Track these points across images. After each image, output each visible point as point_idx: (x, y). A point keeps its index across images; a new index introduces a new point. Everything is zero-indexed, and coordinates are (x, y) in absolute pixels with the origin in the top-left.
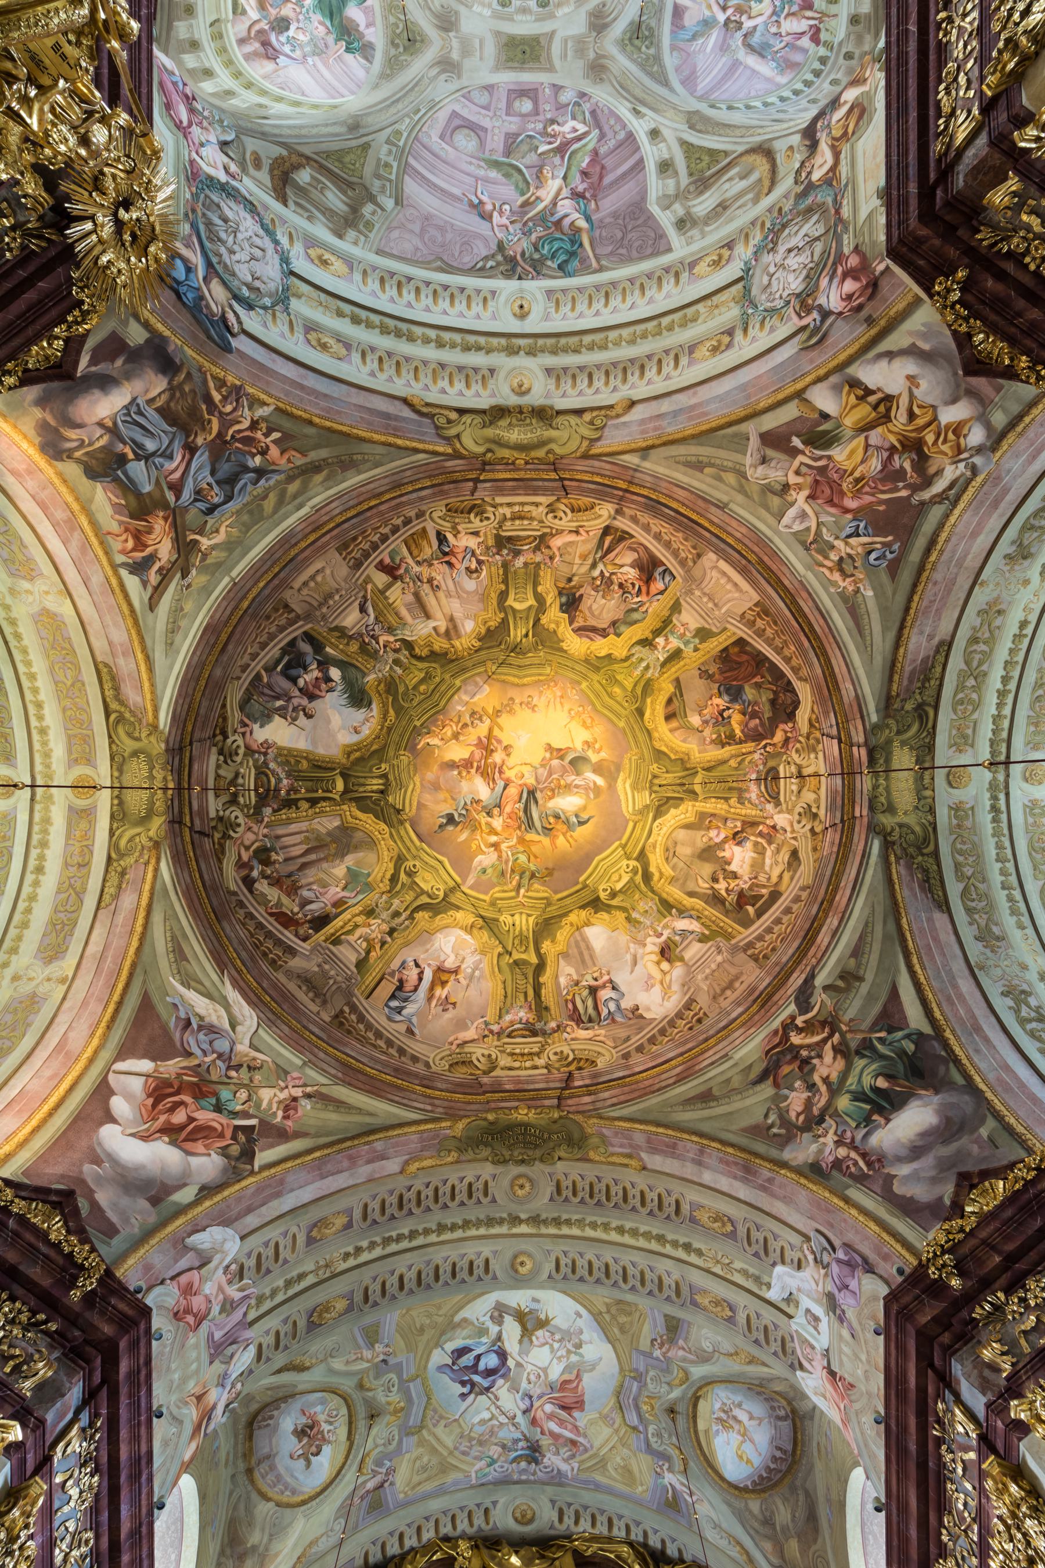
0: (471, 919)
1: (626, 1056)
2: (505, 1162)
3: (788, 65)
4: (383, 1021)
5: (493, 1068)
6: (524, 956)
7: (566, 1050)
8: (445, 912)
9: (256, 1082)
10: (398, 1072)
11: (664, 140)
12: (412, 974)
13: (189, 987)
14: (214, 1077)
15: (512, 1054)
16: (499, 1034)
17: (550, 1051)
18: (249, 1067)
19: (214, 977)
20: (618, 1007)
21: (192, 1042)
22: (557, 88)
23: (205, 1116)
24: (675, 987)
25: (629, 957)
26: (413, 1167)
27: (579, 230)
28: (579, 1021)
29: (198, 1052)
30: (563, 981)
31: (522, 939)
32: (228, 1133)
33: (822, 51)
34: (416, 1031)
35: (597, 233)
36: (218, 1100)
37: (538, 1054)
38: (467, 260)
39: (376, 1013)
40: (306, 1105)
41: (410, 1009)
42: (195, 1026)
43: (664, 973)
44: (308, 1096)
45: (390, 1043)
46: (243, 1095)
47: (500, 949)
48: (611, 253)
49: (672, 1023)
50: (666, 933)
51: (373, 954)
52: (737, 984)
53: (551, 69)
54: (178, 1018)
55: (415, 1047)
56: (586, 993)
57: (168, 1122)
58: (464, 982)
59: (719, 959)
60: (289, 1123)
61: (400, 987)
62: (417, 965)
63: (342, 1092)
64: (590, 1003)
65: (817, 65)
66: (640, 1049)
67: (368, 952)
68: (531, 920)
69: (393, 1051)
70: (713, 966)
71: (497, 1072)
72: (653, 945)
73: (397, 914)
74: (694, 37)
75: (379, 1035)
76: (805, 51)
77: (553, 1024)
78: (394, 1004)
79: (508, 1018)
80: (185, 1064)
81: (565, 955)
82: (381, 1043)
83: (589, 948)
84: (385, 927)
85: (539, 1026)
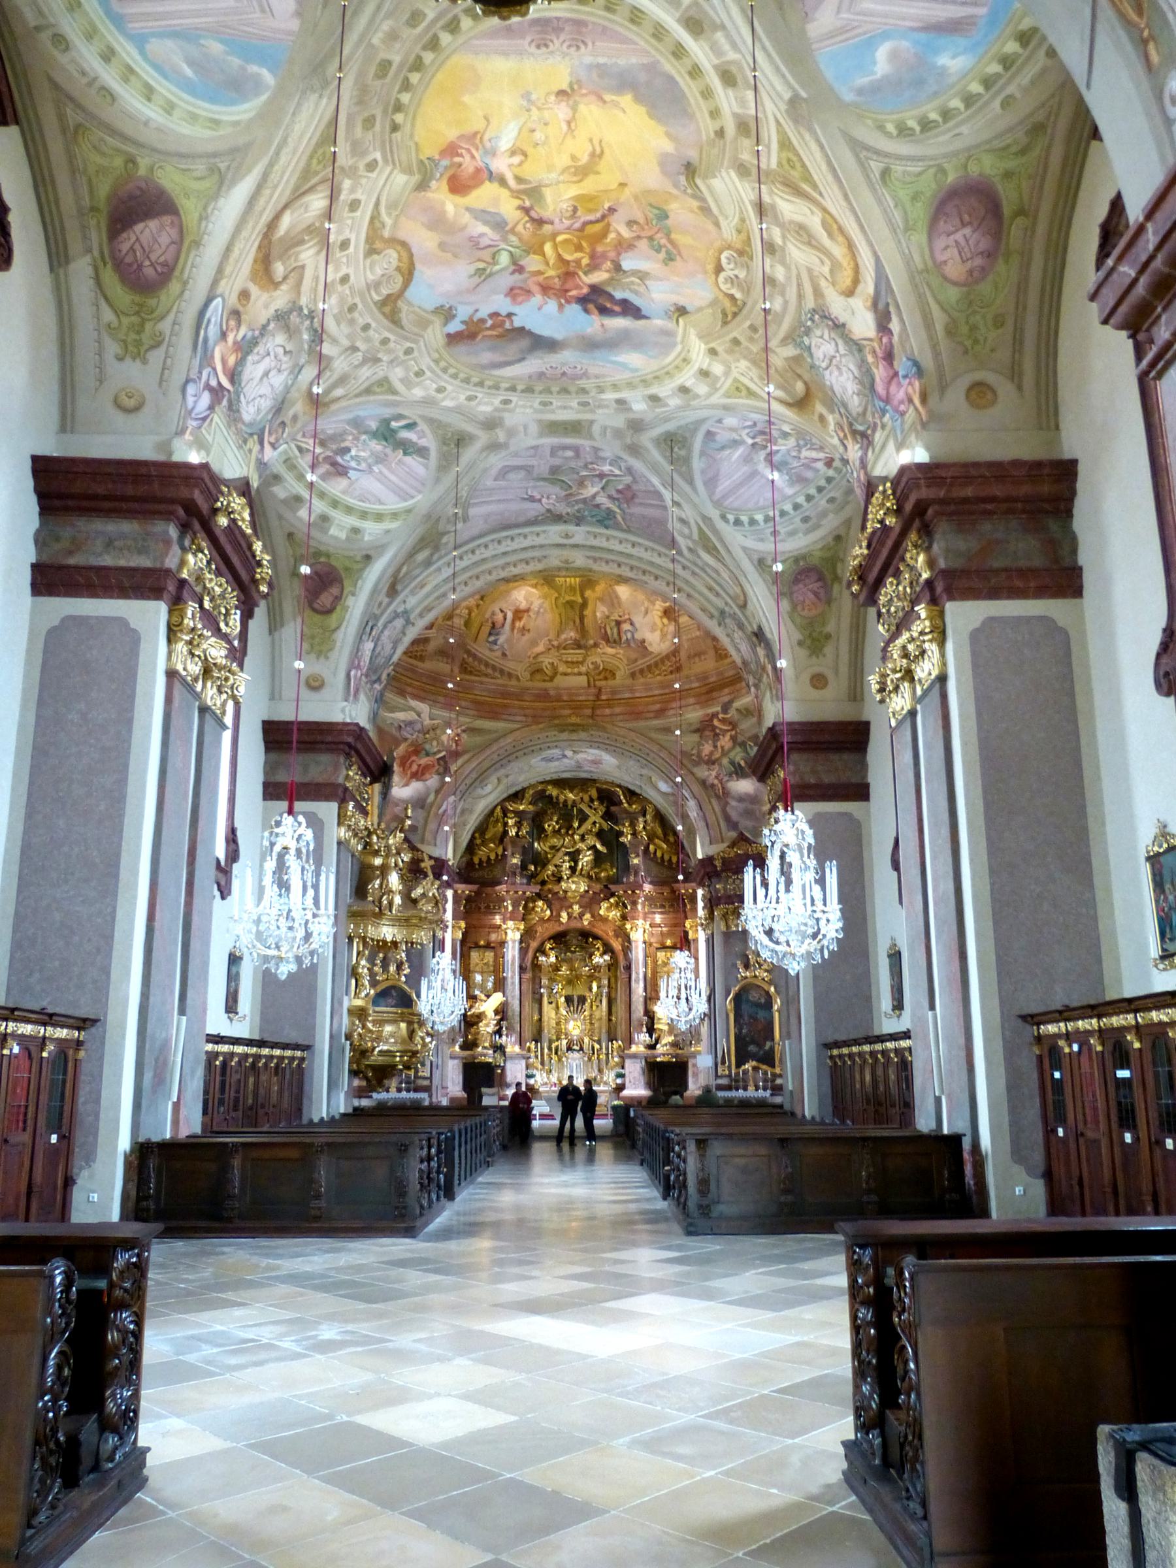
3: (799, 480)
4: (487, 653)
5: (555, 674)
7: (599, 661)
10: (505, 695)
12: (500, 616)
16: (558, 648)
22: (596, 450)
23: (424, 761)
28: (608, 641)
31: (572, 589)
33: (831, 473)
37: (582, 663)
38: (521, 519)
39: (482, 650)
40: (464, 736)
41: (502, 639)
45: (494, 668)
49: (662, 661)
53: (591, 438)
55: (510, 665)
61: (494, 625)
63: (480, 723)
65: (823, 483)
66: (642, 671)
69: (497, 674)
71: (560, 681)
72: (659, 605)
74: (723, 448)
75: (487, 665)
76: (817, 471)
77: (591, 642)
78: (492, 639)
79: (563, 637)
81: (601, 599)
82: (490, 671)
83: (617, 597)
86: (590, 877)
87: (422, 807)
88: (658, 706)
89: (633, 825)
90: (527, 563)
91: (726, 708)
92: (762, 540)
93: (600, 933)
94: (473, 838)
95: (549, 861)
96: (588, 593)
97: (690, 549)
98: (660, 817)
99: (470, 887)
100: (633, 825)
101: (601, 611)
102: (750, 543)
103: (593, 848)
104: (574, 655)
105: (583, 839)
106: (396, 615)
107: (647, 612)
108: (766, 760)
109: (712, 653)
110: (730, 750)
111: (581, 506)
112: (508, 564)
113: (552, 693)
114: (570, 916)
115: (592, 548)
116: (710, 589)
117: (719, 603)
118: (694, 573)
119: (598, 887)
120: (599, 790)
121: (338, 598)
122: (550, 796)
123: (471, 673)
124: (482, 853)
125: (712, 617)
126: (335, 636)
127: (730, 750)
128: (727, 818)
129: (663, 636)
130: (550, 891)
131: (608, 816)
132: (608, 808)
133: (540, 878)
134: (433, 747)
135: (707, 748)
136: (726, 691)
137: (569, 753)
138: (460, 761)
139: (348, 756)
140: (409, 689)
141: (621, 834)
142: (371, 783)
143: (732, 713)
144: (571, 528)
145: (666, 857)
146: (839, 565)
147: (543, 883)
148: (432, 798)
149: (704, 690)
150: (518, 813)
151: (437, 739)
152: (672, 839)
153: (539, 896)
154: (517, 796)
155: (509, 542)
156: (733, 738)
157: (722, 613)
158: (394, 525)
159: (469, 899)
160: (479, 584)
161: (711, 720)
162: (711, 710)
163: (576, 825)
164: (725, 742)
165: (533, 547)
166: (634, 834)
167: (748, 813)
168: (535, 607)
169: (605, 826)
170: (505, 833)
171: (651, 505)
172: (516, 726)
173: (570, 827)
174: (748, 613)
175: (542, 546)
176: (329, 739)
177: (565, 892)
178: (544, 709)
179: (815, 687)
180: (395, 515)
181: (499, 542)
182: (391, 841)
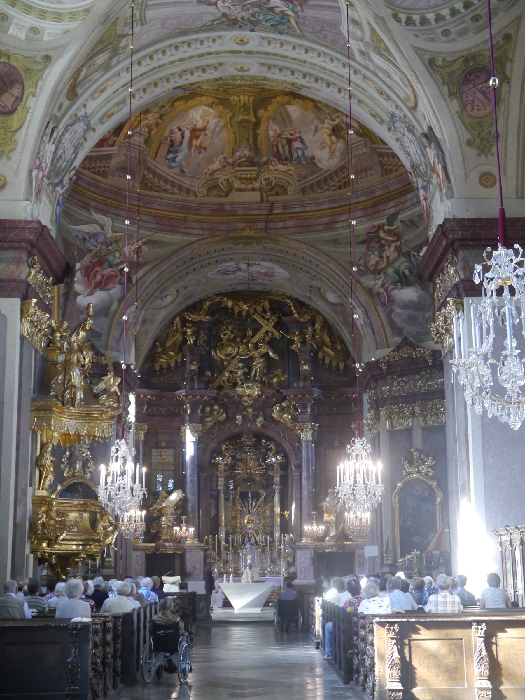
0: (211, 100)
1: (303, 191)
2: (239, 244)
6: (246, 117)
7: (271, 177)
8: (194, 98)
9: (121, 246)
11: (357, 12)
12: (178, 135)
13: (77, 225)
14: (103, 253)
15: (241, 179)
16: (233, 165)
17: (262, 177)
18: (116, 242)
19: (87, 215)
20: (303, 153)
21: (89, 245)
23: (107, 271)
24: (337, 154)
25: (313, 127)
26: (196, 251)
27: (288, 15)
28: (279, 159)
29: (93, 248)
30: (271, 133)
31: (245, 108)
32: (118, 274)
34: (185, 170)
35: (302, 21)
36: (109, 262)
37: (255, 179)
38: (198, 24)
40: (145, 248)
41: (180, 157)
42: (87, 238)
43: (333, 143)
44: (144, 243)
45: (173, 184)
46: (117, 254)
47: (231, 114)
48: (312, 32)
49: (331, 176)
50: (337, 121)
51: (153, 132)
52: (369, 173)
54: (80, 239)
55: (186, 182)
56: (285, 142)
57: (96, 282)
58: (209, 135)
59: (365, 150)
60: (140, 259)
61: (172, 144)
62: (180, 130)
63: (160, 236)
64: (287, 148)
66: (311, 187)
67: (149, 133)
68: (251, 98)
69: (176, 190)
70: (361, 152)
72: (328, 124)
73: (163, 106)
75: (166, 181)
77: (265, 159)
78: (170, 156)
79: (238, 154)
80: (91, 255)
81: (273, 118)
82: (168, 187)
83: (289, 116)
84: (157, 116)
85: (256, 159)
86: (262, 382)
87: (106, 315)
88: (327, 220)
89: (302, 333)
90: (204, 71)
91: (391, 219)
92: (433, 40)
93: (272, 434)
94: (154, 347)
95: (225, 369)
96: (261, 112)
97: (362, 53)
98: (328, 327)
99: (151, 391)
100: (302, 333)
101: (273, 129)
102: (422, 44)
103: (267, 354)
104: (249, 172)
105: (256, 347)
106: (77, 119)
107: (316, 131)
108: (435, 259)
109: (378, 168)
110: (395, 260)
111: (256, 9)
112: (185, 71)
113: (228, 207)
114: (244, 418)
115: (268, 54)
116: (381, 93)
117: (390, 107)
118: (365, 77)
119: (270, 392)
120: (271, 302)
121: (19, 99)
122: (226, 308)
123: (151, 189)
124: (163, 360)
125: (382, 122)
126: (16, 137)
127: (395, 260)
128: (392, 323)
129: (332, 154)
130: (226, 395)
131: (278, 325)
132: (279, 318)
133: (216, 384)
134: (116, 258)
135: (373, 259)
136: (392, 204)
137: (243, 266)
138: (141, 272)
139: (30, 254)
140: (93, 203)
141: (292, 342)
142: (54, 284)
143: (397, 225)
144: (246, 34)
145: (334, 364)
146: (508, 64)
147: (220, 388)
148: (114, 307)
149: (370, 203)
150: (194, 323)
151: (120, 250)
152: (339, 347)
153: (216, 400)
154: (194, 308)
155: (186, 48)
156: (398, 249)
157: (393, 116)
158: (73, 25)
159: (150, 404)
160: (158, 91)
161: (378, 232)
162: (376, 223)
163: (250, 334)
164: (390, 252)
165: (209, 54)
166: (304, 342)
167: (411, 320)
168: (211, 125)
169: (277, 335)
170: (185, 341)
171: (325, 7)
172: (195, 239)
173: (244, 336)
174: (419, 115)
175: (218, 53)
176: (12, 236)
177: (240, 396)
178: (220, 223)
179: (483, 185)
180: (73, 15)
181: (176, 48)
182: (74, 338)
